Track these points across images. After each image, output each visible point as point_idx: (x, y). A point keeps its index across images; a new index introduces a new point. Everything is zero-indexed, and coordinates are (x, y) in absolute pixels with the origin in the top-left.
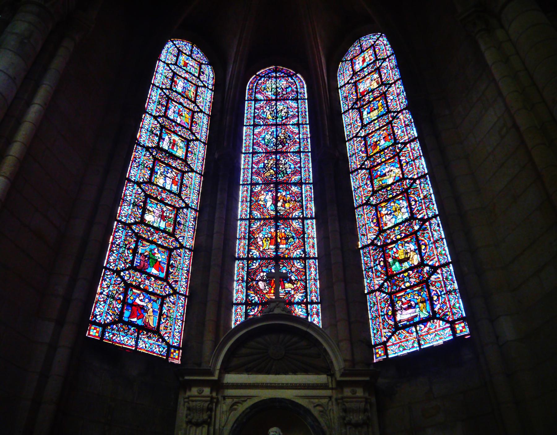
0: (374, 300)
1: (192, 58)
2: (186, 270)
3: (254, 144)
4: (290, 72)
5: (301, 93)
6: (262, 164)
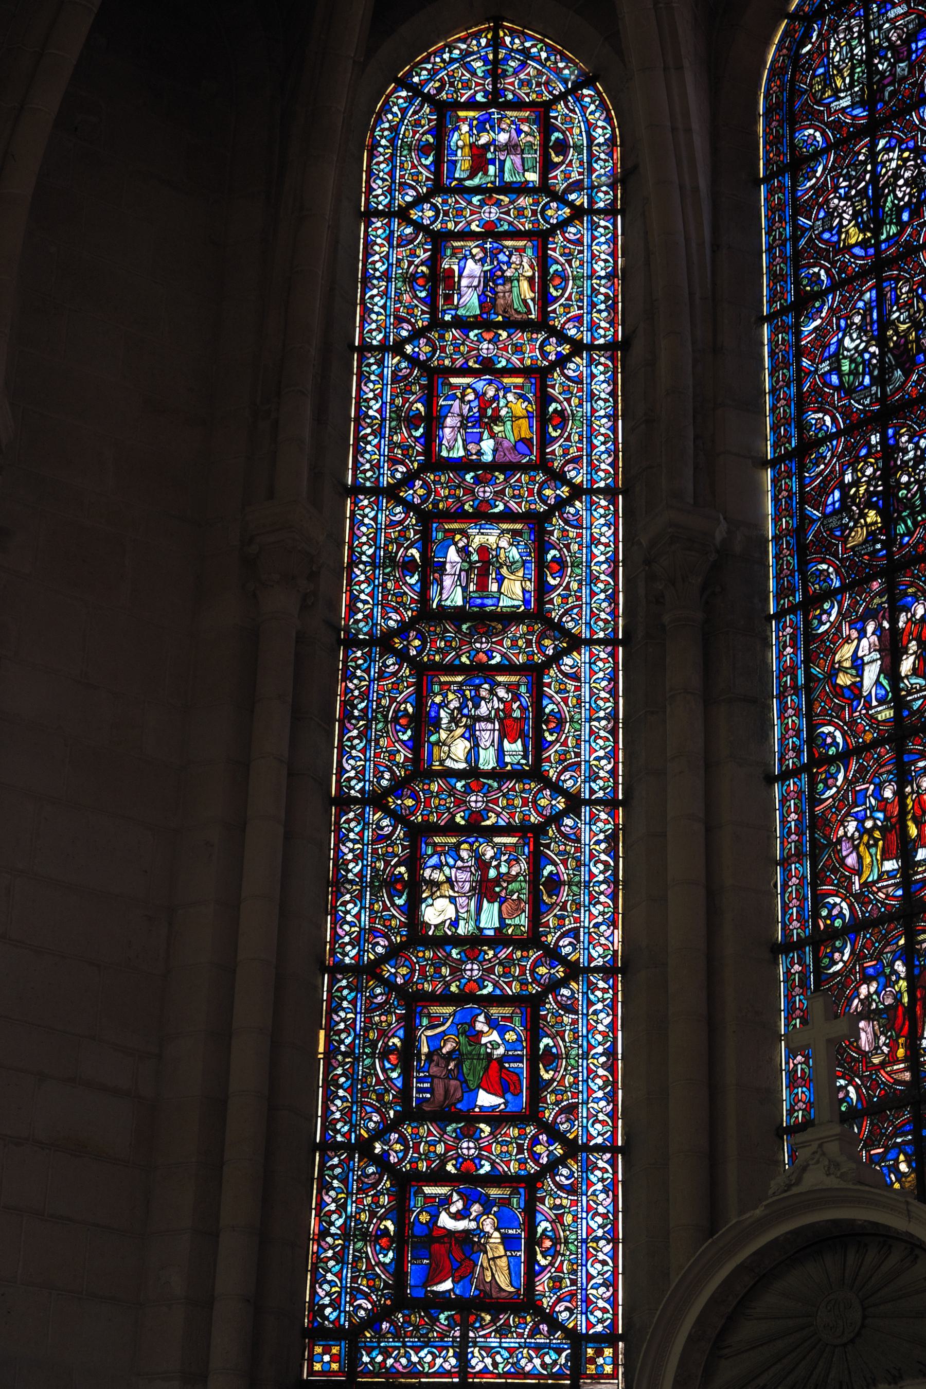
2: (602, 1055)
6: (837, 494)
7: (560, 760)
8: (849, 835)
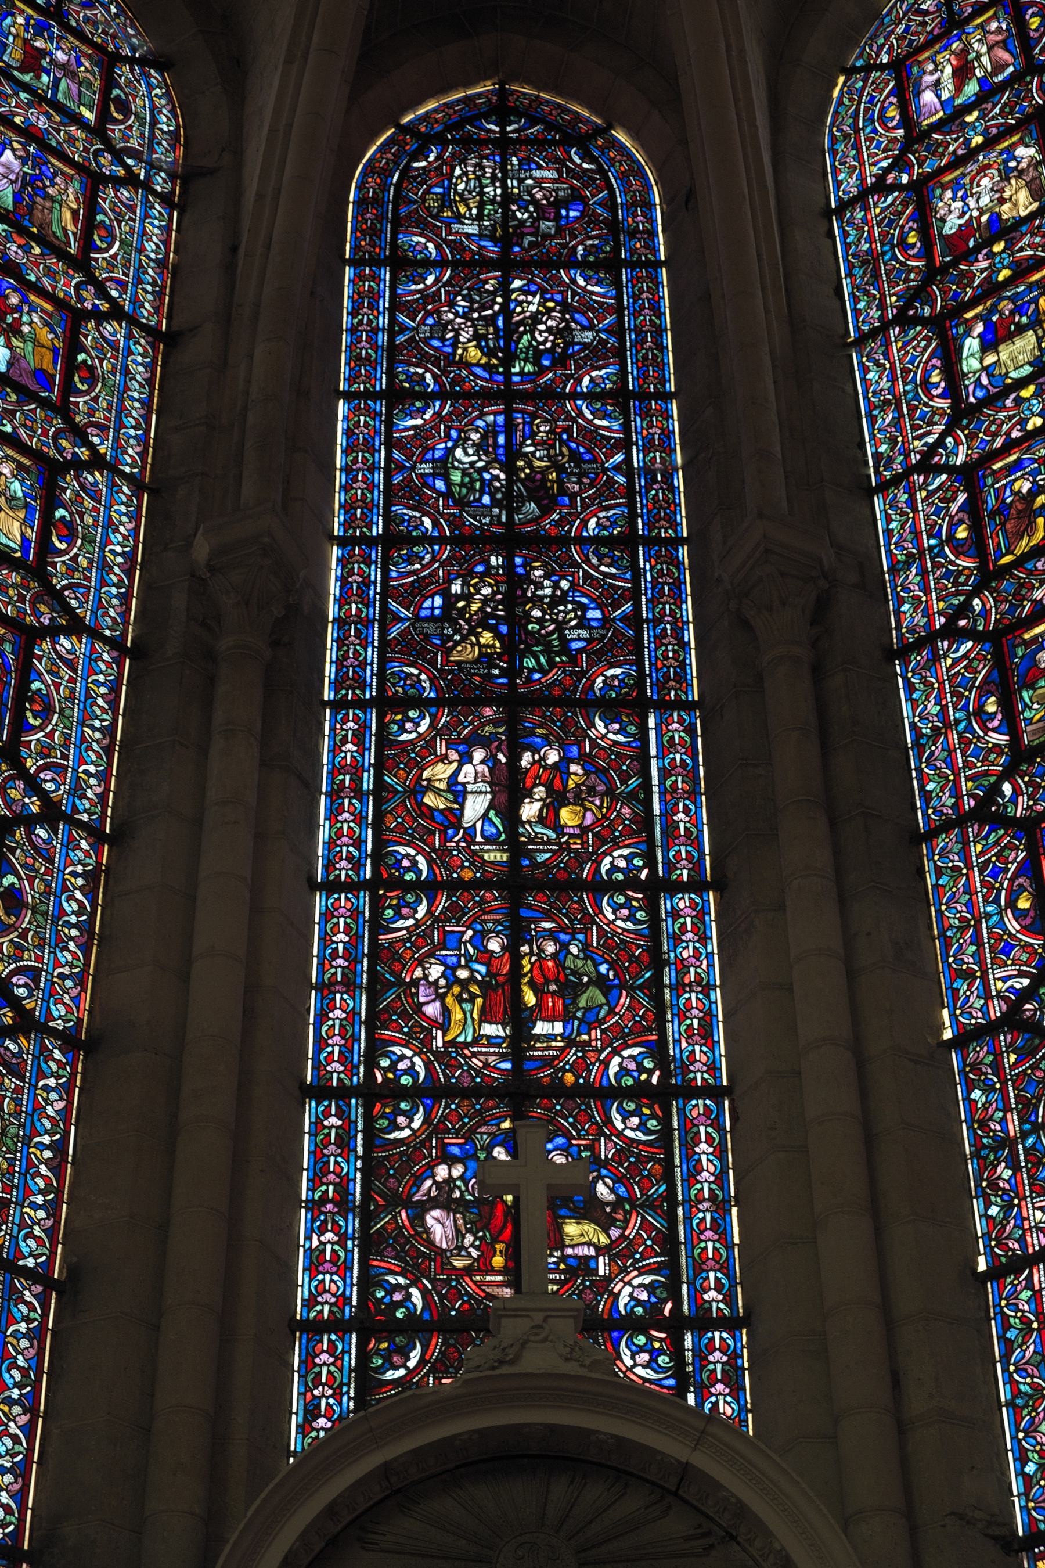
0: (1026, 1308)
1: (65, 27)
3: (390, 493)
4: (577, 116)
5: (633, 233)
6: (438, 601)
7: (42, 752)
8: (431, 979)
